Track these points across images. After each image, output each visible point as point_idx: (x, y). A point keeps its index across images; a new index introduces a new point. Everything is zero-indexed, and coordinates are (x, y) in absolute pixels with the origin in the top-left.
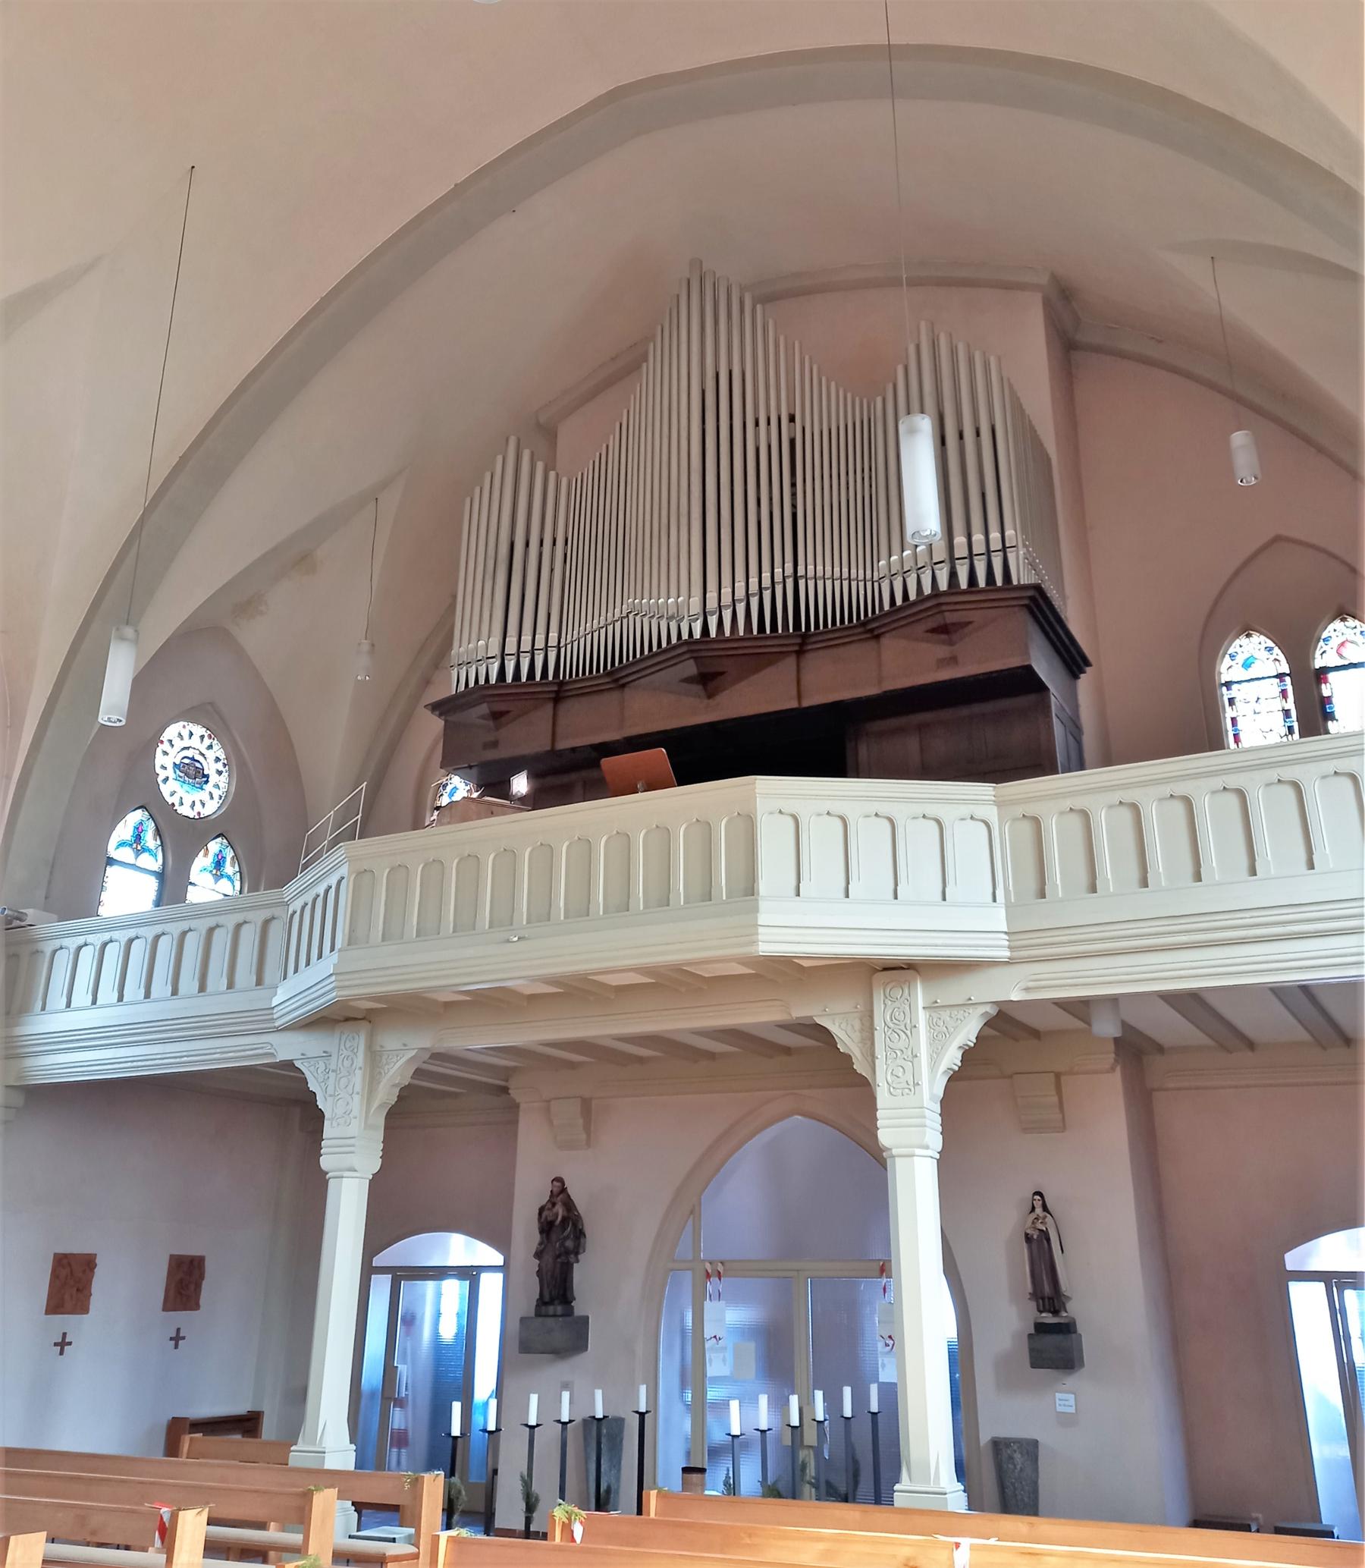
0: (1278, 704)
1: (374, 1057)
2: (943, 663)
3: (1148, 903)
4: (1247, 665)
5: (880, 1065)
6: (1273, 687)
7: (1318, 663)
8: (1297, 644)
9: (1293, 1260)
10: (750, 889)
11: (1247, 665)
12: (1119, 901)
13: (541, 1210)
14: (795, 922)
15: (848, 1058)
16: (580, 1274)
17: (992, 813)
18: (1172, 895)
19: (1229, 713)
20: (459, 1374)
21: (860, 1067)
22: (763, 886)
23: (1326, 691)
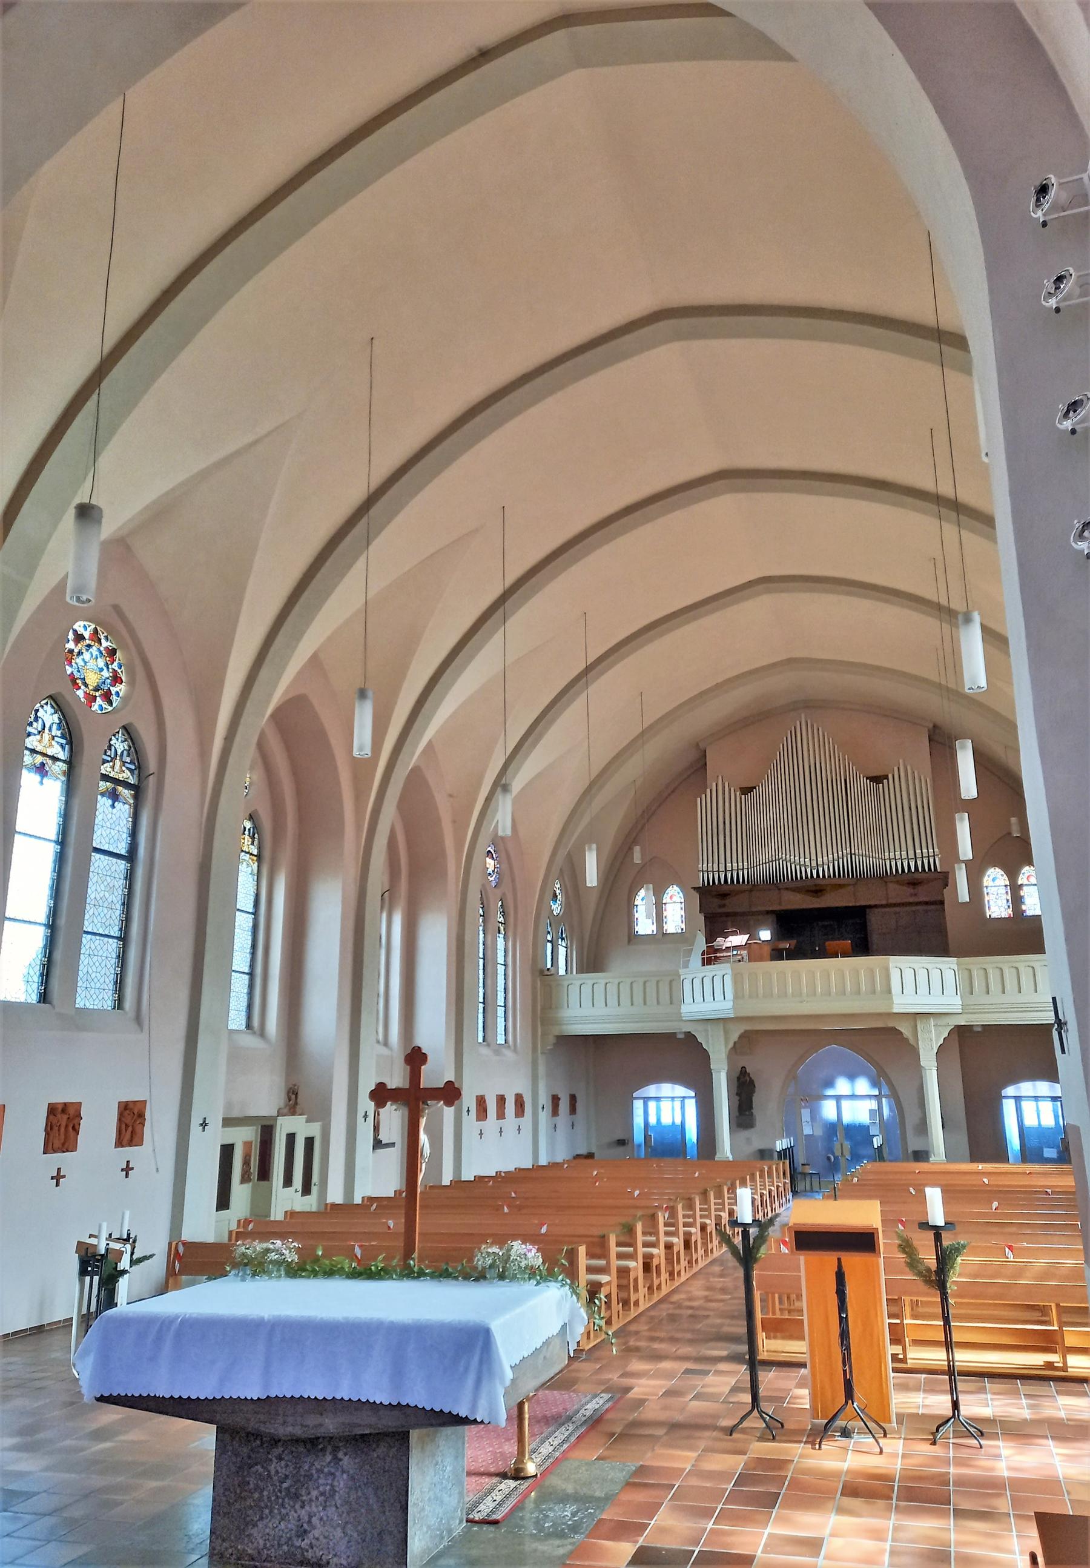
0: (1004, 897)
1: (726, 1032)
2: (911, 895)
3: (1005, 999)
4: (994, 880)
5: (920, 1043)
6: (1003, 890)
7: (1020, 883)
8: (1012, 874)
9: (1010, 1091)
10: (889, 991)
11: (994, 880)
12: (995, 997)
13: (738, 1078)
14: (903, 1001)
15: (907, 1040)
16: (756, 1099)
17: (955, 967)
18: (1011, 997)
19: (987, 898)
20: (679, 1136)
21: (912, 1041)
22: (893, 991)
23: (1022, 893)
